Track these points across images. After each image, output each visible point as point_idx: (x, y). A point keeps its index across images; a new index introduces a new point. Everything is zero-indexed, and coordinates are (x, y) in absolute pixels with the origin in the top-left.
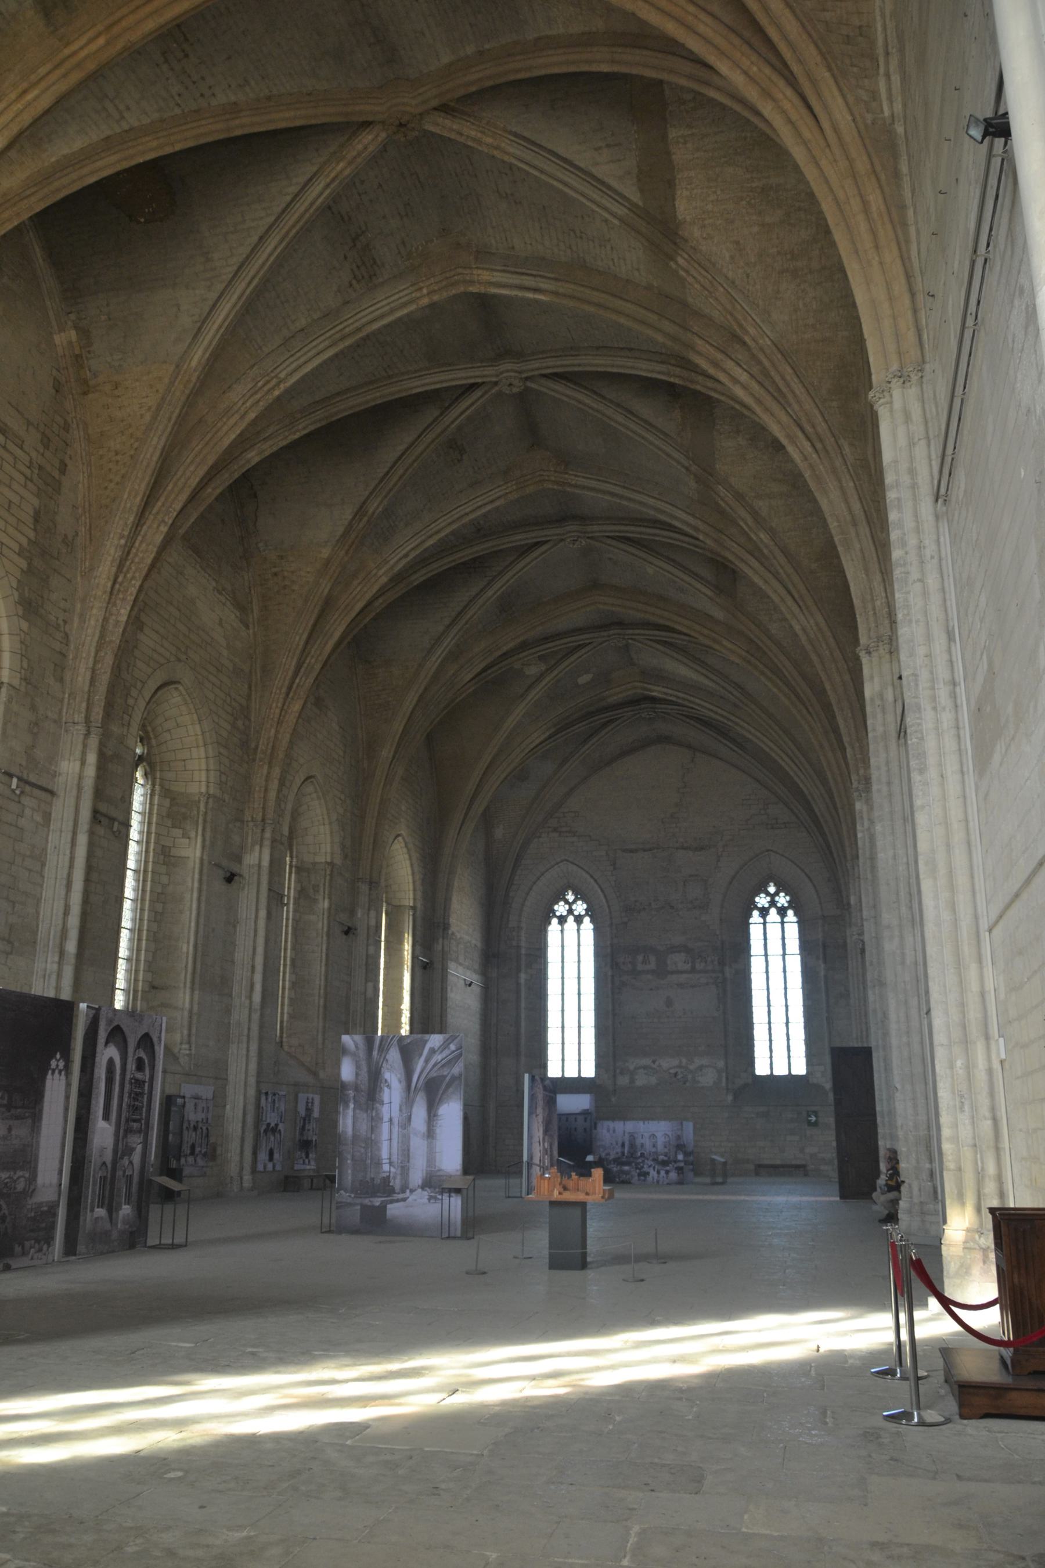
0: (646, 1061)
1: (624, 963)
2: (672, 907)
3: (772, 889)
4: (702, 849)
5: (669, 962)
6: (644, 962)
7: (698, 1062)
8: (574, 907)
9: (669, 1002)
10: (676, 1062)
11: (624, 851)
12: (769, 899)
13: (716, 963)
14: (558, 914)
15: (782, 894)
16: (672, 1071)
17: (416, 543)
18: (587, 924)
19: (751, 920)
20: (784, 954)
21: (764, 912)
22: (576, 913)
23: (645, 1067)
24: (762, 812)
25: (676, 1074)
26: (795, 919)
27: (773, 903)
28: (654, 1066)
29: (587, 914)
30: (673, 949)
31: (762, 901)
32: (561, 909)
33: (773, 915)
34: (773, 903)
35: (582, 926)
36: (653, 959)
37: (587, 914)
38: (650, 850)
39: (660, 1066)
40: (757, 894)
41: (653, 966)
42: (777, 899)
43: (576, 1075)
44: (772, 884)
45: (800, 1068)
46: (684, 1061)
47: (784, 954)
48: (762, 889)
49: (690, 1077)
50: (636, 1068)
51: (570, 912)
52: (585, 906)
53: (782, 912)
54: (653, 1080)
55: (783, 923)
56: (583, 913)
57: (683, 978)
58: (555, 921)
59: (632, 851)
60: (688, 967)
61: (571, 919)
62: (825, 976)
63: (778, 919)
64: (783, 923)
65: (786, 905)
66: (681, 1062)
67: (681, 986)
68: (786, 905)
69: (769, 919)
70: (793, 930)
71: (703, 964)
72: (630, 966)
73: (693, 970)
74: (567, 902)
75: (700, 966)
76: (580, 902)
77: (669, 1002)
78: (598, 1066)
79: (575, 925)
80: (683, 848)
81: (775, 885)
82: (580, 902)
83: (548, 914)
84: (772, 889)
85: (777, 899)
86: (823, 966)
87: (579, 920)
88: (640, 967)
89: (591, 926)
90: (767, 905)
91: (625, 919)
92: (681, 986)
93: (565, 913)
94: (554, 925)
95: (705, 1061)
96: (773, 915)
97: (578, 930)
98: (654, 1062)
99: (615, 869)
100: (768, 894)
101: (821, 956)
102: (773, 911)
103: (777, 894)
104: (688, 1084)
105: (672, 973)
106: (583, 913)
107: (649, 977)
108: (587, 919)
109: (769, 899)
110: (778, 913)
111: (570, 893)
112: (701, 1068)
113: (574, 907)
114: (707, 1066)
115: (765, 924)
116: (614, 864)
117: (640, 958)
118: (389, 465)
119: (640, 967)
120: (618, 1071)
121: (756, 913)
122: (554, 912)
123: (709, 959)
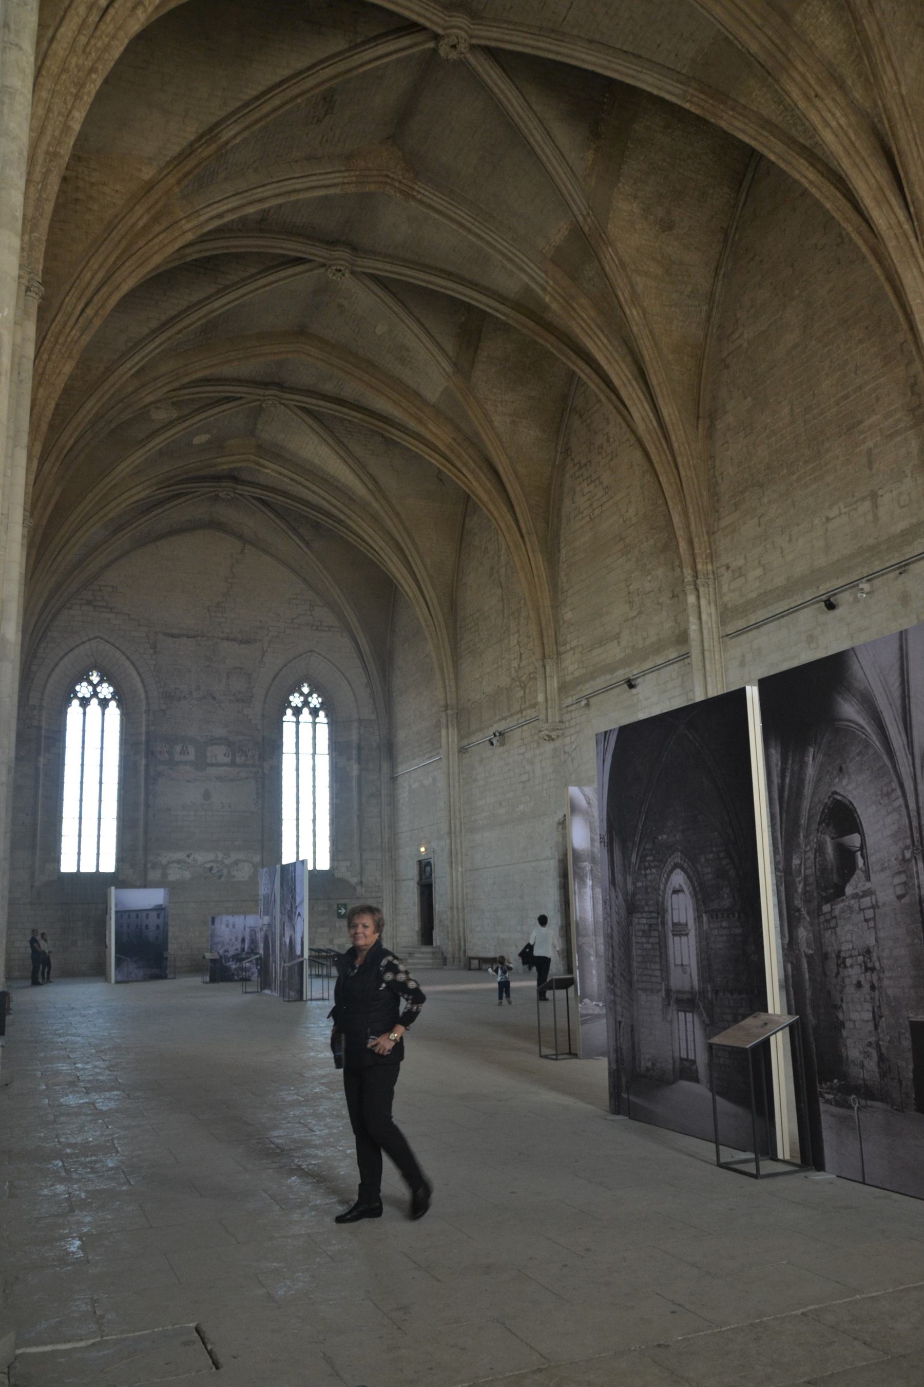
0: (181, 855)
1: (160, 752)
2: (214, 698)
3: (306, 690)
4: (248, 642)
5: (208, 754)
6: (182, 753)
7: (234, 856)
8: (99, 689)
9: (207, 795)
10: (211, 856)
11: (165, 634)
12: (302, 699)
14: (80, 695)
15: (315, 696)
16: (209, 865)
17: (235, 204)
18: (113, 711)
19: (285, 718)
20: (314, 754)
21: (297, 712)
22: (101, 696)
23: (179, 862)
24: (308, 613)
25: (211, 869)
26: (325, 720)
27: (306, 703)
28: (189, 860)
29: (113, 698)
30: (213, 741)
31: (296, 700)
32: (83, 690)
33: (306, 715)
34: (306, 703)
35: (107, 711)
36: (192, 750)
37: (113, 698)
38: (194, 637)
39: (195, 860)
40: (292, 693)
41: (191, 757)
42: (310, 699)
43: (74, 870)
44: (306, 685)
45: (324, 864)
46: (220, 855)
47: (314, 754)
48: (297, 689)
49: (225, 871)
50: (169, 863)
51: (95, 694)
52: (111, 689)
53: (314, 712)
54: (187, 875)
55: (298, 723)
56: (109, 696)
57: (222, 771)
58: (75, 703)
59: (173, 636)
60: (227, 760)
61: (94, 701)
62: (359, 778)
63: (310, 719)
64: (314, 724)
65: (318, 706)
66: (217, 857)
67: (219, 778)
68: (318, 706)
69: (301, 718)
70: (323, 731)
71: (243, 758)
72: (167, 756)
73: (233, 764)
74: (90, 683)
75: (238, 760)
76: (105, 685)
77: (207, 795)
78: (120, 860)
79: (99, 709)
80: (227, 639)
81: (309, 686)
82: (105, 685)
83: (69, 695)
84: (306, 690)
85: (310, 699)
86: (356, 767)
87: (104, 703)
88: (177, 758)
89: (118, 712)
90: (300, 705)
91: (164, 707)
92: (219, 778)
93: (88, 696)
94: (74, 709)
95: (241, 856)
96: (306, 715)
97: (103, 714)
98: (188, 856)
99: (155, 653)
100: (302, 694)
101: (354, 757)
102: (306, 711)
103: (310, 694)
104: (223, 879)
105: (212, 765)
106: (109, 696)
108: (113, 704)
109: (302, 699)
110: (310, 713)
111: (95, 674)
112: (236, 862)
113: (99, 689)
114: (244, 861)
115: (298, 723)
116: (155, 647)
117: (178, 748)
118: (261, 88)
119: (177, 758)
120: (149, 865)
121: (289, 712)
122: (75, 693)
123: (250, 754)
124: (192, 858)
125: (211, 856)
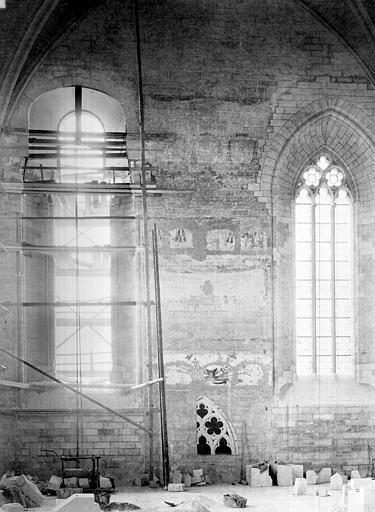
5: (208, 239)
7: (240, 357)
9: (208, 288)
10: (215, 358)
13: (265, 243)
16: (211, 368)
23: (178, 364)
28: (190, 362)
36: (189, 236)
39: (196, 362)
41: (189, 243)
54: (188, 379)
60: (230, 246)
73: (237, 251)
77: (208, 288)
80: (227, 99)
92: (222, 269)
95: (250, 357)
98: (189, 358)
105: (213, 253)
107: (186, 256)
114: (250, 363)
123: (257, 239)
124: (192, 359)
125: (215, 358)
